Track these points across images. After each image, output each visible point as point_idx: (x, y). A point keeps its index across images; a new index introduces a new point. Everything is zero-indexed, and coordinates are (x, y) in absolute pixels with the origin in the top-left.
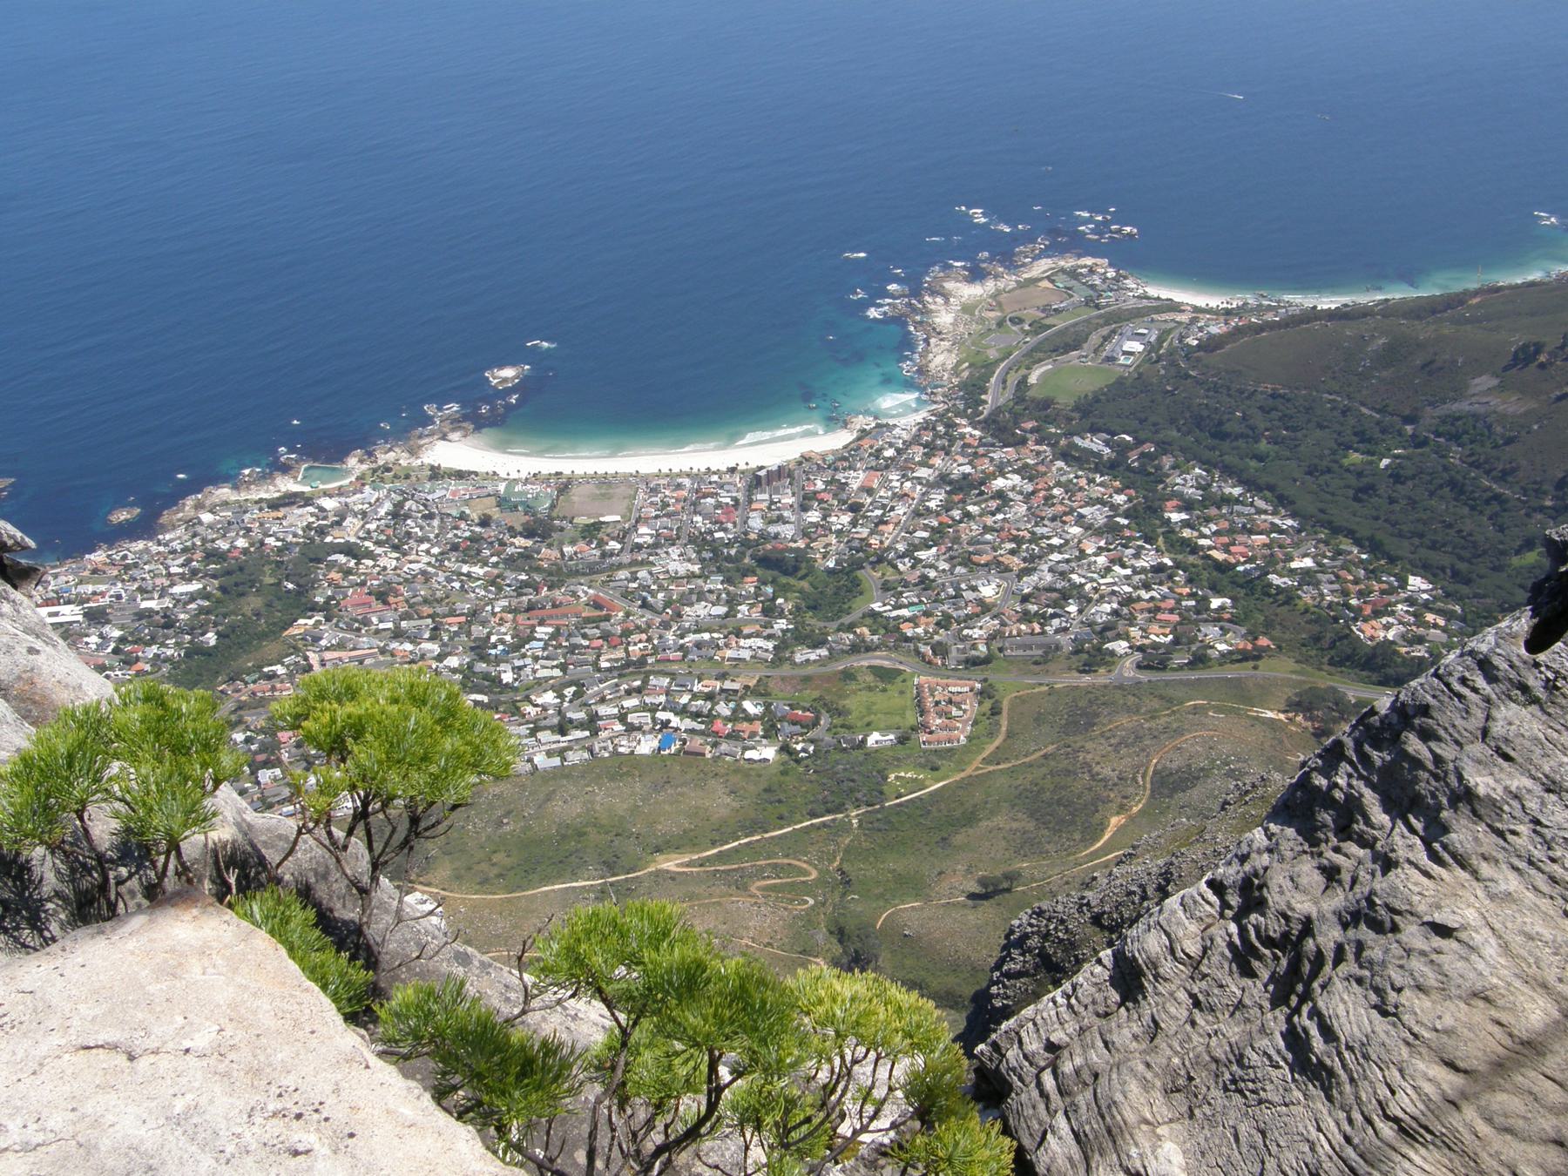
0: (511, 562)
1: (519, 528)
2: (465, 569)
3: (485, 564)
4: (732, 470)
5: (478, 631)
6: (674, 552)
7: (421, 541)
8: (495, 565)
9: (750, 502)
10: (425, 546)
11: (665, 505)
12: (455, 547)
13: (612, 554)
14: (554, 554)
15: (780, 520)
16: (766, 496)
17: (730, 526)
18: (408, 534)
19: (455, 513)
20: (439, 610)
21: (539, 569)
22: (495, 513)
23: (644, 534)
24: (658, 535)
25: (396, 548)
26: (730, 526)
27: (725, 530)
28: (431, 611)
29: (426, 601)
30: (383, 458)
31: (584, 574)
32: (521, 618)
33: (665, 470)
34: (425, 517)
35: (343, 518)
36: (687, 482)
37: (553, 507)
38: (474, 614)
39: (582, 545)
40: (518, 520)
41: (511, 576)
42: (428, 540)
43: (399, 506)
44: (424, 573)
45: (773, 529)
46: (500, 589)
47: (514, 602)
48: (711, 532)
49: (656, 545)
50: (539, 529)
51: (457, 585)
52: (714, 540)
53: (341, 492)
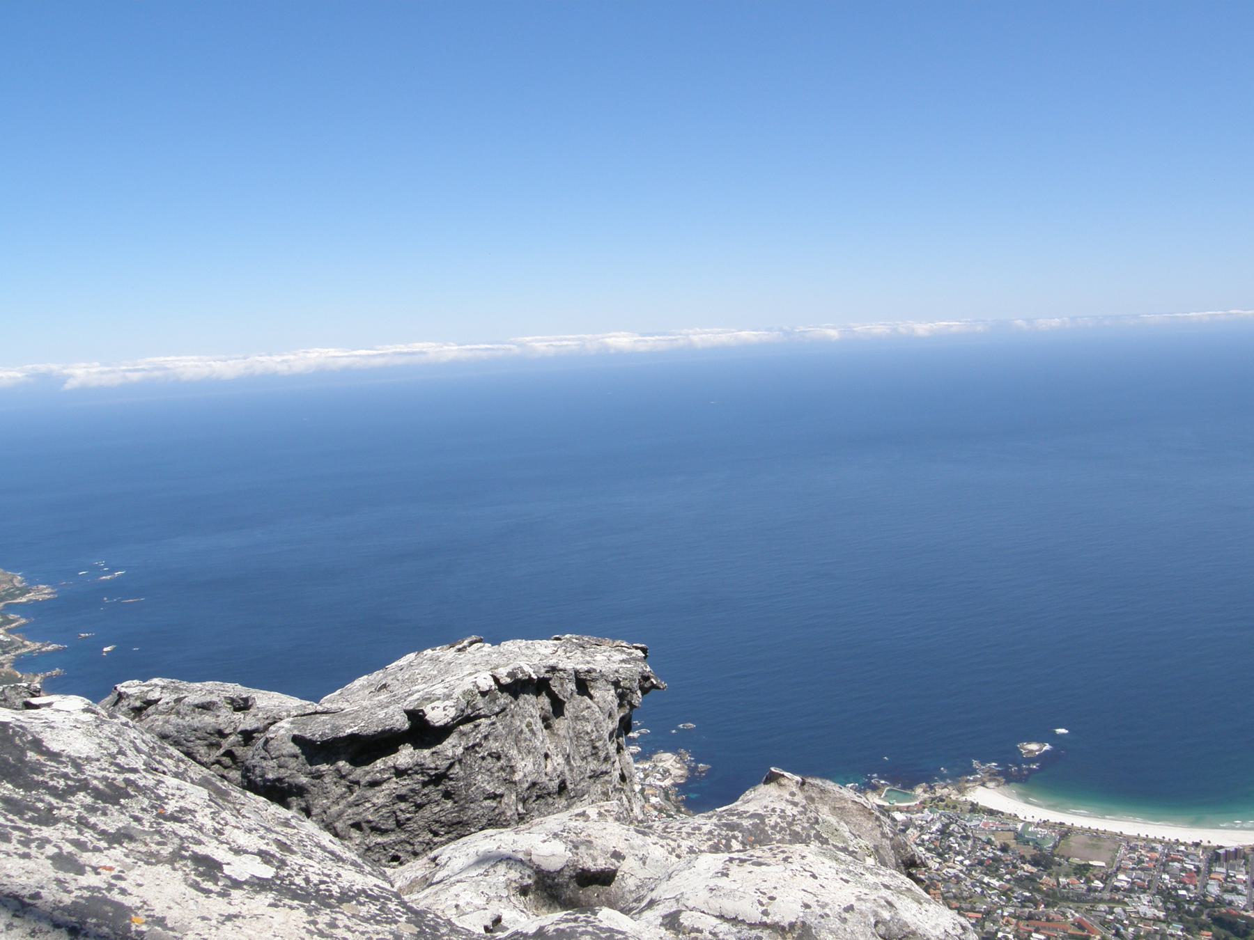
0: (1020, 881)
1: (1029, 858)
2: (986, 879)
3: (1001, 878)
4: (1197, 845)
5: (989, 926)
6: (1145, 898)
7: (958, 853)
8: (1008, 881)
9: (1210, 872)
10: (960, 858)
11: (1140, 861)
12: (981, 863)
13: (1095, 890)
14: (1052, 881)
15: (1234, 890)
16: (1223, 870)
17: (1192, 887)
18: (950, 848)
19: (984, 838)
20: (964, 905)
21: (1039, 891)
22: (1013, 844)
23: (1122, 880)
24: (1133, 883)
25: (940, 855)
26: (1192, 887)
27: (1188, 890)
28: (958, 905)
29: (955, 897)
30: (940, 792)
31: (1073, 901)
32: (1022, 924)
33: (1143, 835)
34: (962, 837)
35: (907, 828)
36: (1159, 847)
37: (1055, 847)
38: (988, 913)
39: (1073, 879)
40: (1029, 851)
41: (1018, 891)
42: (963, 854)
43: (946, 826)
44: (956, 876)
45: (1228, 897)
46: (1009, 899)
47: (1019, 911)
48: (1175, 889)
49: (1131, 890)
50: (1043, 861)
51: (979, 890)
52: (1178, 895)
53: (908, 810)
